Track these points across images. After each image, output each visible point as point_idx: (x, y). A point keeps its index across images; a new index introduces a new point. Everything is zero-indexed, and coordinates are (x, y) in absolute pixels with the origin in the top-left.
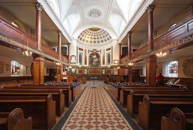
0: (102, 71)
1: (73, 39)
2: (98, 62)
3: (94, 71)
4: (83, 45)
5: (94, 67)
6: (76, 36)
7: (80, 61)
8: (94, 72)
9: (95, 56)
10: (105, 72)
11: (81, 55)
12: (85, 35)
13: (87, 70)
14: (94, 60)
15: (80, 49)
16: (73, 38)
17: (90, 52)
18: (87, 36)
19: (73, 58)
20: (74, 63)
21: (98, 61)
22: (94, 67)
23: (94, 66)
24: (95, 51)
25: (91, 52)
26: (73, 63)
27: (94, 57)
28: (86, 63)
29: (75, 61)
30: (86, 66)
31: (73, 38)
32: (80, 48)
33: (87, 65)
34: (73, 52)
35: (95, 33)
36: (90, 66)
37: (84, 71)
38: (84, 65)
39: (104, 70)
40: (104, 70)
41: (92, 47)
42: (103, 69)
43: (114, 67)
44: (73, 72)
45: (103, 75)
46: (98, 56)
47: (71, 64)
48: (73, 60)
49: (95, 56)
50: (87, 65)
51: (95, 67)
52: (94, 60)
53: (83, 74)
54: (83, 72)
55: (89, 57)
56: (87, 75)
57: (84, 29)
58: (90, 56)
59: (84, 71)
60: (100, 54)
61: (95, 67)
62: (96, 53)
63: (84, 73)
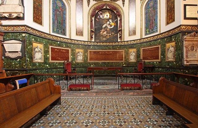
0: (127, 54)
2: (117, 30)
5: (105, 44)
8: (106, 56)
9: (107, 15)
10: (138, 56)
13: (86, 52)
14: (104, 26)
20: (18, 18)
21: (116, 26)
22: (105, 44)
23: (106, 42)
27: (105, 17)
29: (19, 9)
33: (85, 37)
36: (93, 40)
37: (74, 54)
38: (74, 37)
39: (135, 50)
40: (135, 50)
42: (132, 46)
43: (184, 33)
44: (13, 56)
45: (129, 65)
46: (116, 14)
49: (107, 15)
50: (85, 37)
51: (108, 44)
52: (104, 26)
54: (70, 57)
55: (92, 16)
60: (121, 5)
61: (108, 44)
62: (108, 5)
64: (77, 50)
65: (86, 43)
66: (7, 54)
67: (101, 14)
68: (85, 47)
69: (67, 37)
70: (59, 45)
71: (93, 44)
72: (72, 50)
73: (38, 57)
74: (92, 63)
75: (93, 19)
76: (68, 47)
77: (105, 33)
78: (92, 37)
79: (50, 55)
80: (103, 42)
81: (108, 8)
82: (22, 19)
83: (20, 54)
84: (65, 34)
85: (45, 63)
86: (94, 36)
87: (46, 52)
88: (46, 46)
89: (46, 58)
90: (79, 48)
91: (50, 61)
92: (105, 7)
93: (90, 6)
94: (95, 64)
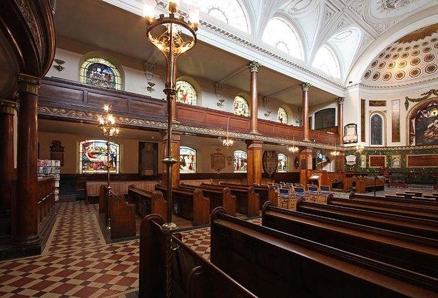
1: (351, 84)
3: (427, 158)
4: (389, 91)
5: (430, 147)
6: (357, 76)
7: (377, 136)
11: (380, 118)
12: (388, 61)
13: (403, 157)
15: (372, 103)
16: (350, 82)
17: (412, 105)
18: (398, 61)
19: (351, 131)
20: (354, 142)
22: (430, 147)
23: (432, 144)
24: (433, 96)
25: (416, 103)
26: (349, 143)
27: (432, 114)
28: (396, 137)
29: (355, 138)
30: (396, 144)
31: (350, 82)
32: (375, 102)
33: (403, 142)
34: (350, 115)
35: (425, 43)
36: (414, 144)
37: (389, 160)
38: (390, 144)
41: (421, 86)
44: (351, 164)
47: (345, 145)
48: (350, 135)
50: (403, 142)
53: (387, 168)
54: (386, 163)
55: (412, 118)
56: (401, 171)
57: (380, 48)
58: (416, 115)
59: (389, 160)
63: (389, 165)
64: (393, 156)
65: (404, 149)
66: (347, 163)
67: (426, 113)
68: (402, 152)
69: (383, 145)
70: (376, 154)
71: (412, 148)
72: (388, 157)
73: (363, 165)
74: (412, 169)
75: (414, 121)
76: (384, 154)
77: (431, 134)
78: (411, 141)
79: (369, 163)
80: (427, 145)
81: (435, 104)
82: (357, 142)
83: (355, 163)
84: (381, 143)
85: (367, 168)
86: (414, 140)
87: (367, 160)
88: (367, 157)
89: (367, 165)
90: (395, 154)
91: (370, 167)
92: (430, 105)
93: (409, 109)
94: (415, 169)
